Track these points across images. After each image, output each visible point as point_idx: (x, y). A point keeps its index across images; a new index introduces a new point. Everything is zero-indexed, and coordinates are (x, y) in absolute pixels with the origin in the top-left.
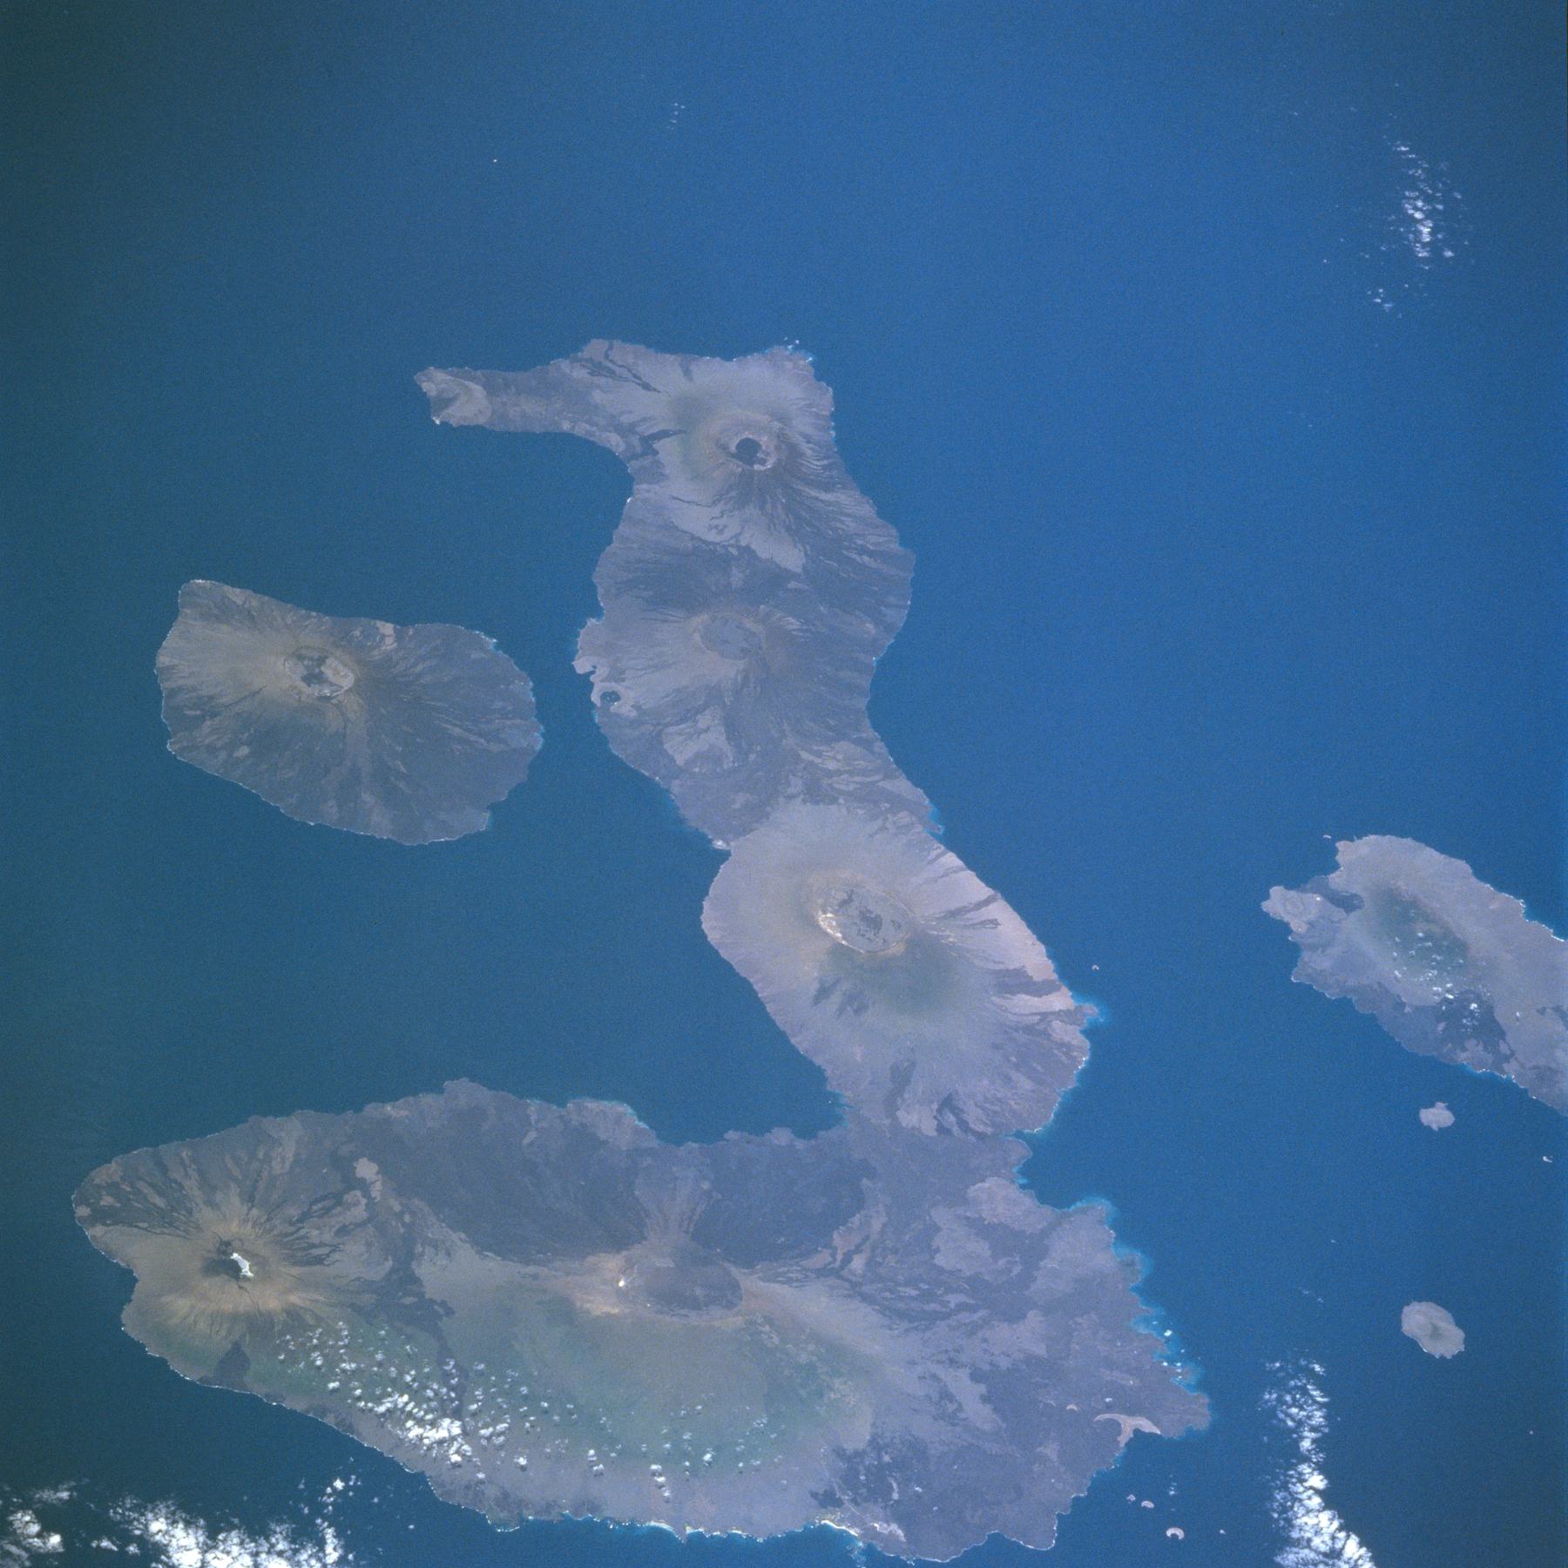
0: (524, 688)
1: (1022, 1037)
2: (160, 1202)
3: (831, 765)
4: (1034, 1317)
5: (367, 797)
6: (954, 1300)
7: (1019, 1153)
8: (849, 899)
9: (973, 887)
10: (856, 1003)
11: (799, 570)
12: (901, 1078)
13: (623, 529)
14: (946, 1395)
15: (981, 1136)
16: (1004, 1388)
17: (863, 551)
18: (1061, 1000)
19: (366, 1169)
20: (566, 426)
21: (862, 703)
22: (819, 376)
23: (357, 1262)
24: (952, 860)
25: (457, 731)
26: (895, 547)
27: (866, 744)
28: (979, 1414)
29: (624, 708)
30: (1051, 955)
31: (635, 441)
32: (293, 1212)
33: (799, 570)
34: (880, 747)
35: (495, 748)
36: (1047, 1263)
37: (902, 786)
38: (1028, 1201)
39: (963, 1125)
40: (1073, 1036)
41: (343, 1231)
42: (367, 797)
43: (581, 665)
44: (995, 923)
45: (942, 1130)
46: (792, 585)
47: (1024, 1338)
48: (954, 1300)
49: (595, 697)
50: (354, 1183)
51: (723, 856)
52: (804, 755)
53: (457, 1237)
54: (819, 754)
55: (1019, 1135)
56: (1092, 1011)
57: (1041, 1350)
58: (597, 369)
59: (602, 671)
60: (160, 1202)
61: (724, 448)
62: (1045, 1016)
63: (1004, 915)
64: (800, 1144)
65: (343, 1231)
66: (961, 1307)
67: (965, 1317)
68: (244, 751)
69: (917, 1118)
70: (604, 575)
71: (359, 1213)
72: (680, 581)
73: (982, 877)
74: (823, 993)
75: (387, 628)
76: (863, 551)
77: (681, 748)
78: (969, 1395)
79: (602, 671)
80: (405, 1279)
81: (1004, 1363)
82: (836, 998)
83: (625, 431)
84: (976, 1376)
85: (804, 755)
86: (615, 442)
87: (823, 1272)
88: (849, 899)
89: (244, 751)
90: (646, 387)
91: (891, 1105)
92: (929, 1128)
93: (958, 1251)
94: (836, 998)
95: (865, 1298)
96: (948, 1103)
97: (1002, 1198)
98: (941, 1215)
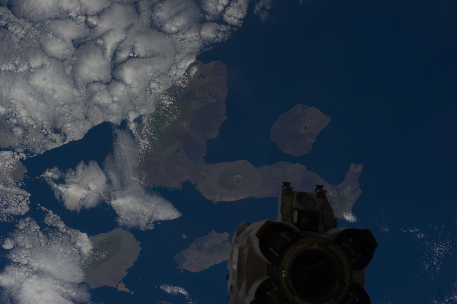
9: (241, 197)
18: (218, 200)
19: (215, 100)
24: (247, 197)
30: (226, 202)
43: (298, 164)
49: (291, 163)
55: (196, 184)
73: (242, 199)
75: (313, 141)
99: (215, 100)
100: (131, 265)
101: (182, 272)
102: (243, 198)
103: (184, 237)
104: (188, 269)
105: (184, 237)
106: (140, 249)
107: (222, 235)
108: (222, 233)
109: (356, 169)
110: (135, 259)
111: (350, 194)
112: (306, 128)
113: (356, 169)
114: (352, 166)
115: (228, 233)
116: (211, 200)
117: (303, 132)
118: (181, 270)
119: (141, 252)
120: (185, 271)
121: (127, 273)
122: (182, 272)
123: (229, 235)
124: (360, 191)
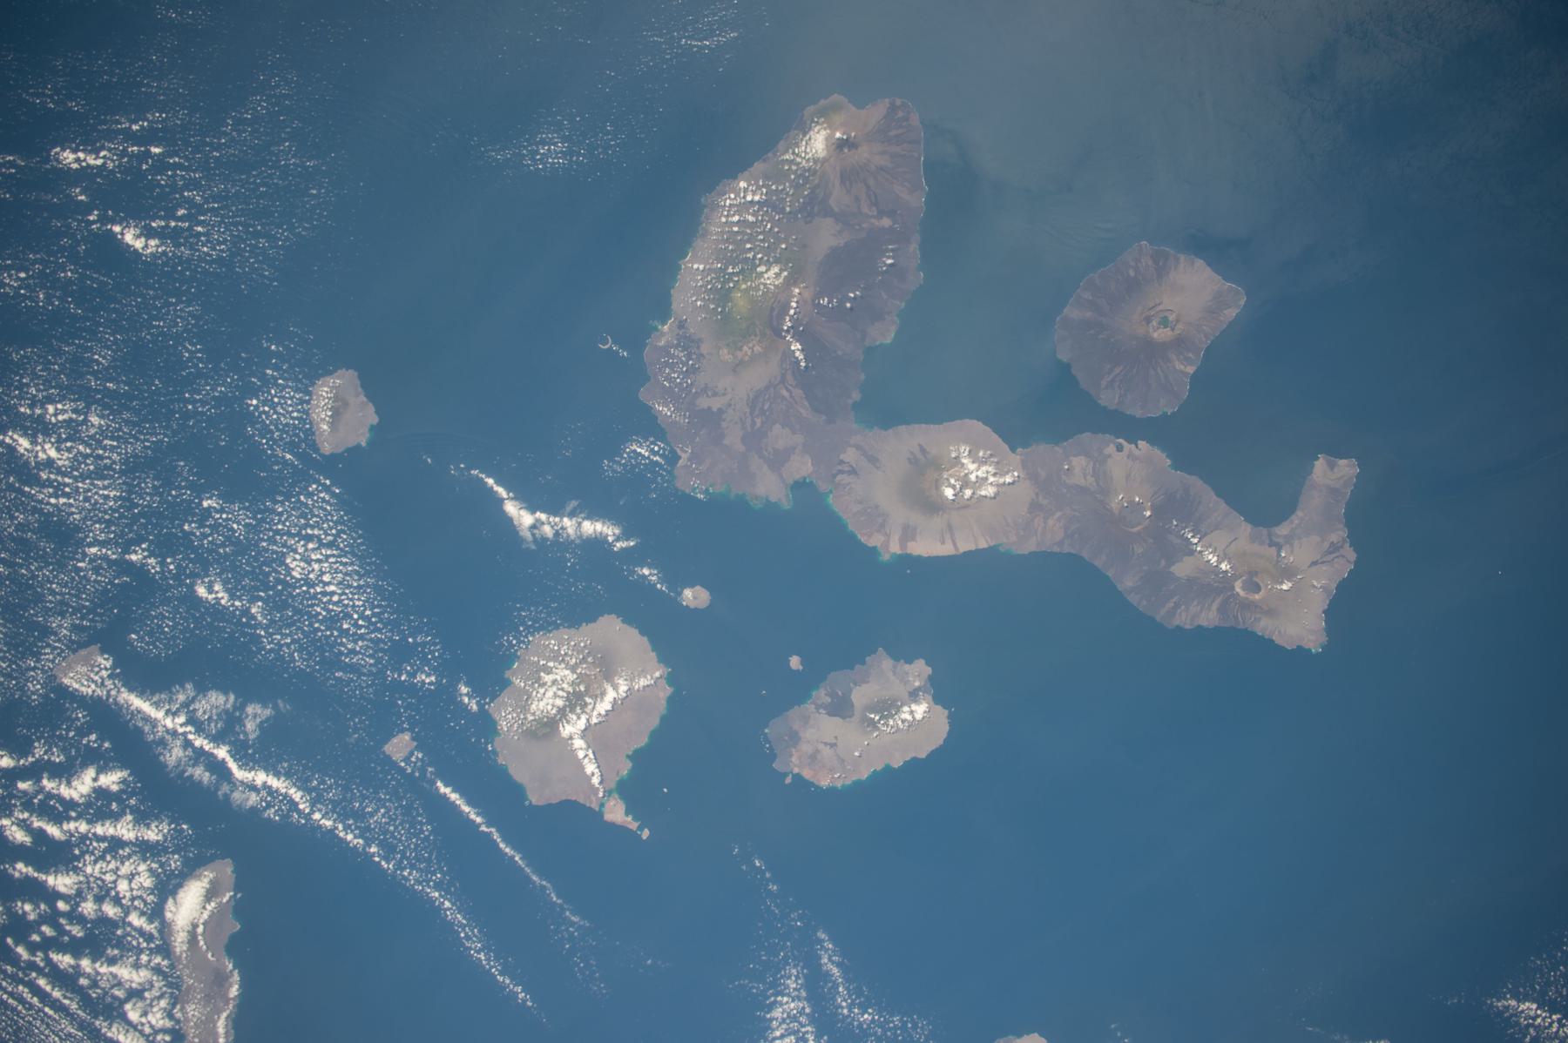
0: (1138, 413)
1: (880, 520)
2: (892, 133)
3: (1051, 522)
4: (742, 448)
5: (1089, 314)
6: (758, 421)
7: (823, 486)
8: (972, 487)
9: (964, 546)
10: (913, 461)
11: (1172, 569)
12: (873, 460)
13: (1223, 505)
14: (715, 394)
15: (834, 476)
16: (711, 419)
17: (1177, 606)
18: (895, 548)
19: (886, 222)
20: (1299, 513)
21: (1085, 554)
22: (1300, 647)
23: (838, 198)
24: (983, 544)
25: (1117, 370)
26: (1176, 622)
27: (1060, 543)
28: (703, 403)
29: (1111, 449)
30: (919, 557)
31: (1281, 540)
32: (871, 182)
33: (1172, 569)
34: (1056, 549)
35: (1104, 383)
36: (765, 468)
37: (1030, 546)
38: (797, 477)
39: (841, 472)
40: (875, 541)
41: (857, 199)
42: (1089, 314)
43: (1141, 443)
44: (943, 543)
45: (842, 462)
46: (1163, 562)
47: (733, 439)
48: (758, 421)
50: (881, 214)
51: (1013, 450)
52: (1058, 514)
53: (842, 242)
54: (1059, 519)
56: (885, 557)
57: (726, 442)
58: (1334, 548)
59: (1136, 452)
60: (892, 133)
61: (1256, 573)
62: (888, 536)
63: (945, 550)
64: (850, 402)
65: (857, 199)
66: (754, 423)
67: (749, 421)
68: (1132, 273)
69: (850, 456)
70: (1195, 482)
71: (865, 210)
72: (1173, 508)
74: (923, 450)
75: (1191, 370)
76: (1177, 606)
77: (1079, 462)
78: (716, 404)
79: (1136, 452)
80: (828, 212)
81: (724, 425)
82: (920, 456)
83: (1289, 539)
84: (720, 410)
85: (1058, 514)
86: (1283, 530)
87: (784, 376)
88: (972, 487)
89: (1132, 273)
90: (1314, 563)
91: (858, 447)
92: (842, 457)
93: (781, 437)
94: (920, 456)
95: (767, 388)
96: (853, 472)
97: (801, 467)
98: (799, 439)
99: (886, 222)
100: (642, 741)
101: (788, 780)
102: (972, 547)
103: (795, 662)
104: (807, 774)
105: (795, 662)
106: (669, 690)
107: (907, 667)
108: (909, 661)
109: (1332, 475)
110: (655, 722)
111: (1314, 563)
112: (1164, 322)
113: (1332, 475)
114: (1320, 465)
115: (928, 664)
116: (875, 548)
117: (1155, 335)
118: (785, 775)
119: (670, 700)
120: (798, 777)
121: (630, 765)
122: (788, 780)
123: (929, 670)
124: (1352, 556)
